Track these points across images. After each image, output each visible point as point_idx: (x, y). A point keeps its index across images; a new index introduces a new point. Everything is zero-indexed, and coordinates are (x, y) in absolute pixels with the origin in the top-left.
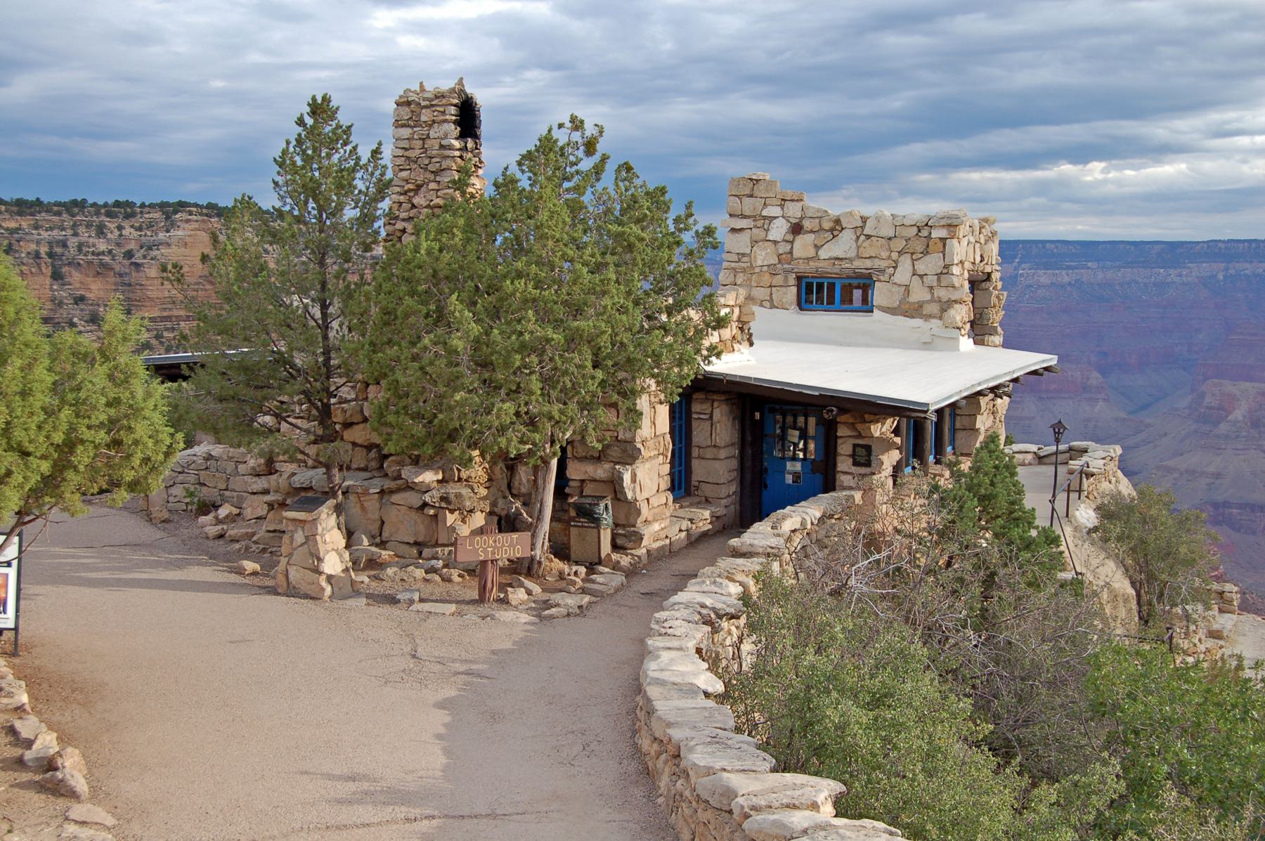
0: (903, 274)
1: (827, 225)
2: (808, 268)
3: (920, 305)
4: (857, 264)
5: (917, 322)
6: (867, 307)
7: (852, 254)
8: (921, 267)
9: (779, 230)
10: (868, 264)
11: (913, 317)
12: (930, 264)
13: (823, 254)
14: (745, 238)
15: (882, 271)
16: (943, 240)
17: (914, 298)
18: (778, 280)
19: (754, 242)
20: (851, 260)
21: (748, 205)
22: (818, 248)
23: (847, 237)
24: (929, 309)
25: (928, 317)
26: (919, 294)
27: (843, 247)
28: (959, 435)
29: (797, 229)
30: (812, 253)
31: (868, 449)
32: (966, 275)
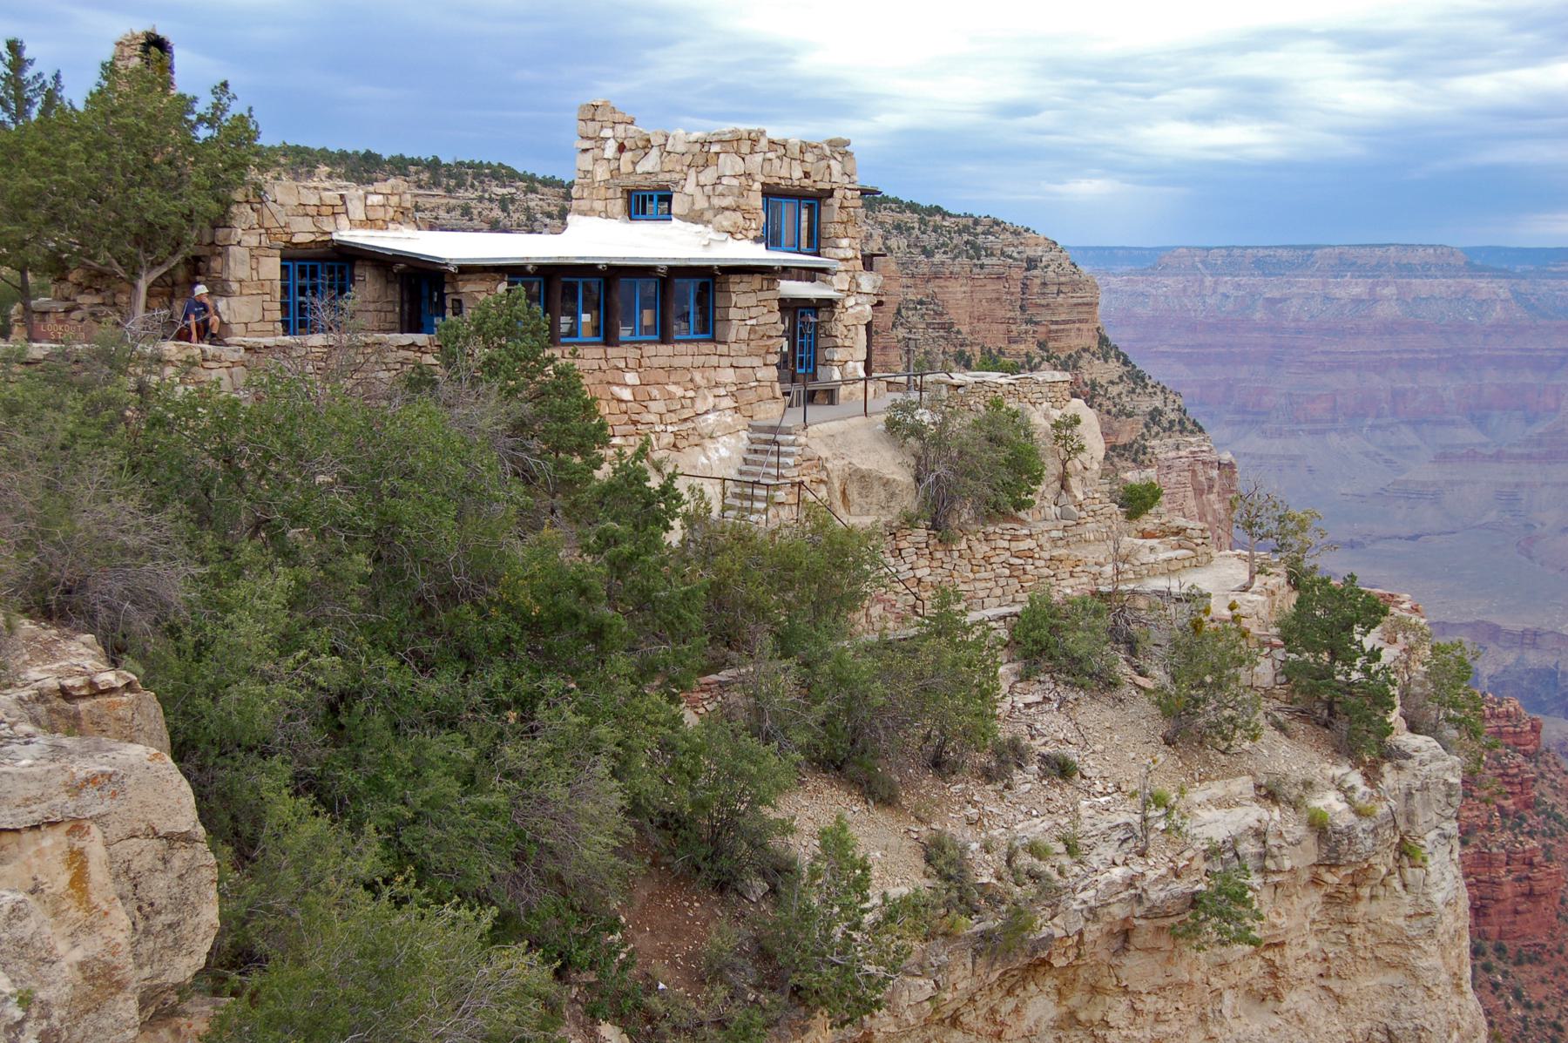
0: (690, 187)
1: (640, 144)
2: (630, 182)
3: (702, 212)
4: (661, 177)
5: (700, 227)
6: (667, 216)
7: (657, 169)
8: (703, 179)
9: (610, 149)
10: (668, 177)
11: (696, 223)
12: (708, 176)
13: (639, 169)
14: (589, 155)
15: (677, 183)
16: (717, 154)
17: (697, 207)
18: (610, 193)
19: (596, 160)
20: (656, 174)
21: (591, 128)
22: (634, 164)
23: (654, 153)
24: (708, 215)
25: (707, 223)
26: (701, 203)
27: (650, 163)
28: (718, 325)
29: (622, 148)
30: (630, 169)
31: (459, 301)
32: (757, 186)
